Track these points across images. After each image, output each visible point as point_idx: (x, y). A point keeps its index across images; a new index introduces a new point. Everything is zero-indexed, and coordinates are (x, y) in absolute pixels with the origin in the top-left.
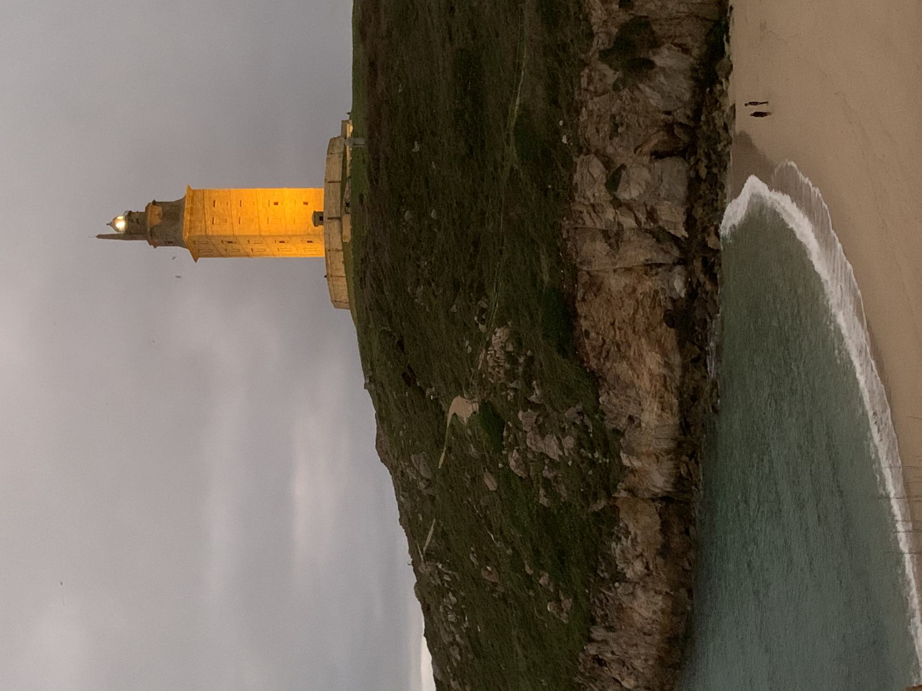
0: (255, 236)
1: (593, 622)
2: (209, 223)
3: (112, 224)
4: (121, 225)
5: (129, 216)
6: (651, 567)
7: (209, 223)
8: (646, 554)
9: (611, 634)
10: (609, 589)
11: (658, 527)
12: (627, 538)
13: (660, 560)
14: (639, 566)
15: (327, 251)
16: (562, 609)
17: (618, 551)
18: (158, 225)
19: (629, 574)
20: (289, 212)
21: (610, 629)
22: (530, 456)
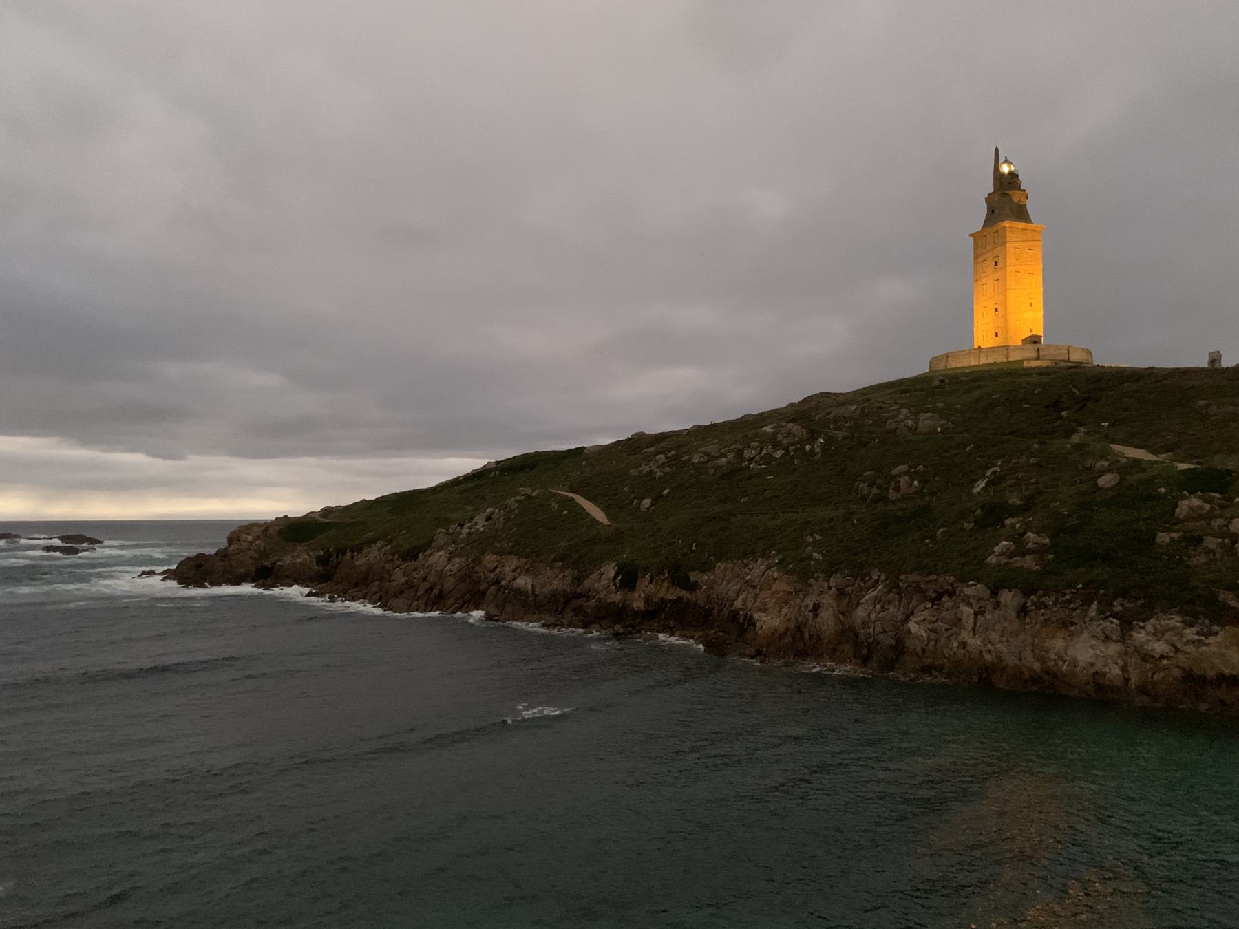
0: (1006, 283)
1: (1027, 593)
2: (1016, 245)
3: (1006, 161)
4: (1005, 169)
5: (1013, 175)
6: (1165, 662)
7: (1016, 245)
8: (1179, 655)
9: (1012, 614)
10: (1100, 612)
11: (1226, 671)
12: (1198, 633)
13: (1177, 673)
14: (1159, 647)
15: (1007, 348)
16: (1010, 558)
17: (1172, 623)
18: (1007, 200)
19: (1140, 636)
20: (1012, 315)
21: (1023, 611)
22: (1220, 521)
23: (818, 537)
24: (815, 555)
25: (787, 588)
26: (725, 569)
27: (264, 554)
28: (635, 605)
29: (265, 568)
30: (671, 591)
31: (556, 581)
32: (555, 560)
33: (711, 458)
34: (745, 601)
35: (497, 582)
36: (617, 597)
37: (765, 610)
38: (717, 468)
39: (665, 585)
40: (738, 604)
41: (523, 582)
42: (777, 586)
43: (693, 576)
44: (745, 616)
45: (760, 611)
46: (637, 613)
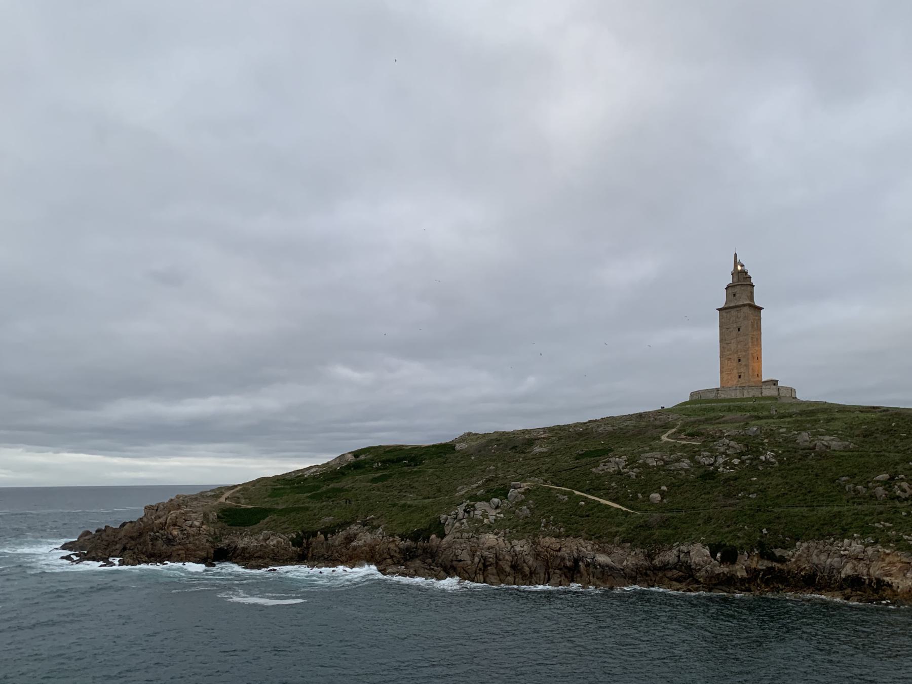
23: (887, 524)
24: (905, 537)
25: (905, 560)
26: (808, 548)
27: (217, 538)
28: (739, 574)
29: (221, 549)
30: (760, 563)
31: (631, 559)
32: (624, 541)
33: (666, 463)
34: (854, 568)
35: (576, 561)
36: (724, 569)
37: (891, 575)
38: (686, 471)
39: (756, 559)
40: (848, 570)
41: (602, 558)
42: (888, 559)
43: (778, 552)
44: (871, 580)
45: (887, 576)
46: (742, 580)
